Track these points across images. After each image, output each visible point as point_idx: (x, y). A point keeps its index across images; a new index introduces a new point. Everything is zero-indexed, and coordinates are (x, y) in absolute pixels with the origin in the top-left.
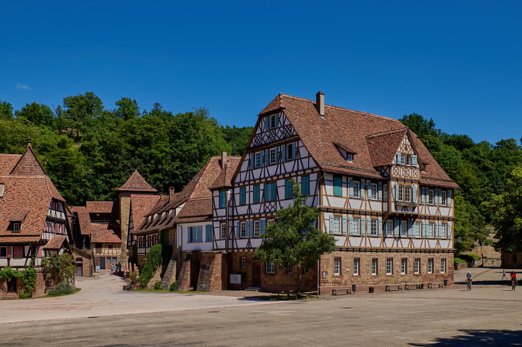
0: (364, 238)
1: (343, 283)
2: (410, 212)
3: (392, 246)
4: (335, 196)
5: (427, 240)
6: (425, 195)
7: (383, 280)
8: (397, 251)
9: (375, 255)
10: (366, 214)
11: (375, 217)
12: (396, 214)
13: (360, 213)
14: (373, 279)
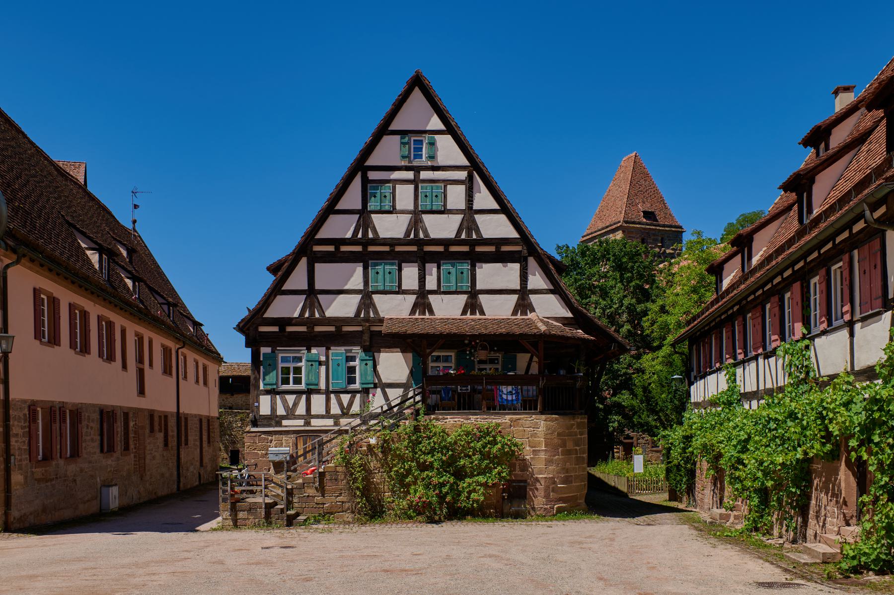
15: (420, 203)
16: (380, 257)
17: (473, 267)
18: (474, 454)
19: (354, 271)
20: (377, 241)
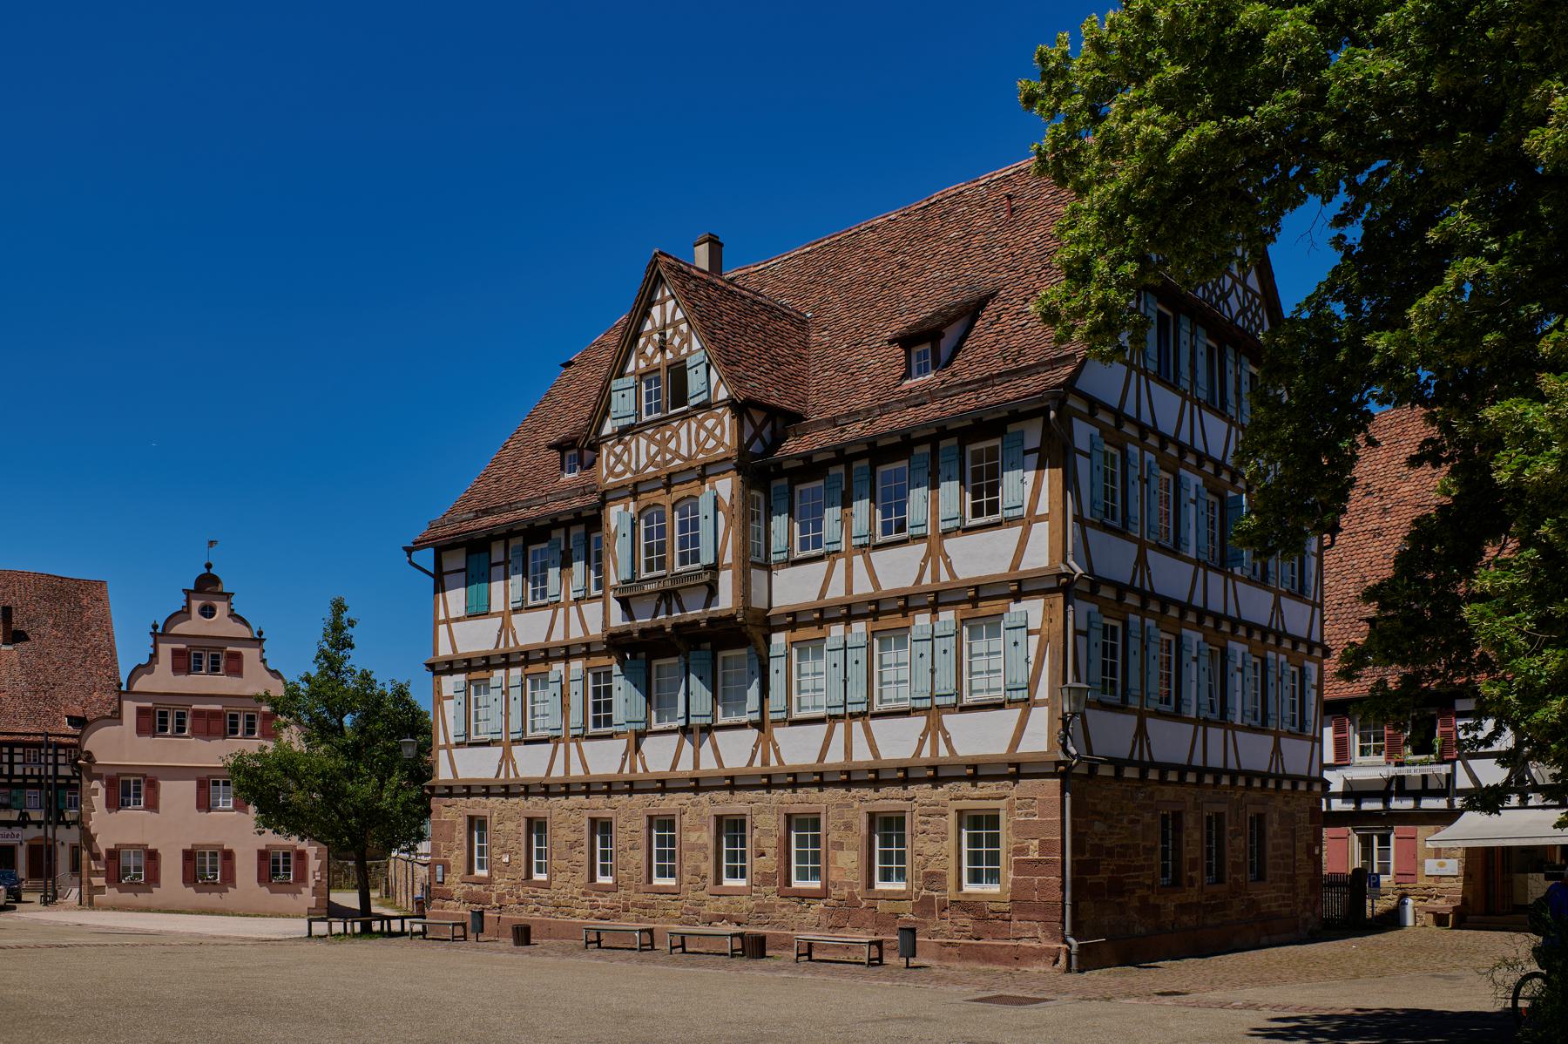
0: (561, 746)
1: (494, 903)
2: (695, 613)
3: (674, 766)
4: (470, 617)
5: (857, 726)
6: (846, 503)
7: (634, 905)
8: (697, 785)
9: (600, 805)
10: (567, 653)
11: (603, 661)
12: (629, 633)
13: (547, 655)
14: (593, 897)
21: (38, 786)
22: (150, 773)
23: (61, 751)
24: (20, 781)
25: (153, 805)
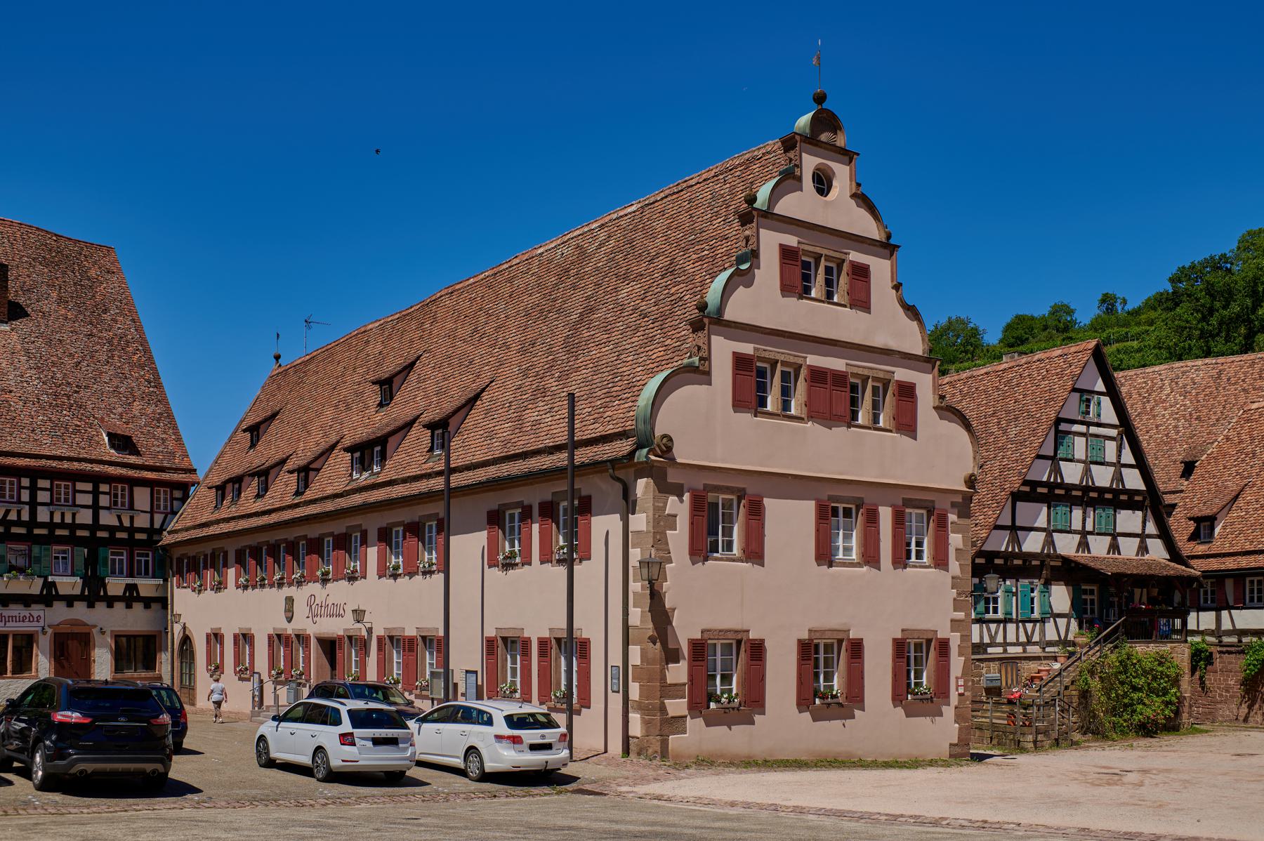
15: (1089, 455)
16: (1060, 499)
17: (1115, 511)
18: (1162, 678)
19: (1041, 510)
20: (1062, 485)
21: (72, 540)
22: (752, 488)
23: (104, 488)
24: (44, 532)
25: (754, 553)
